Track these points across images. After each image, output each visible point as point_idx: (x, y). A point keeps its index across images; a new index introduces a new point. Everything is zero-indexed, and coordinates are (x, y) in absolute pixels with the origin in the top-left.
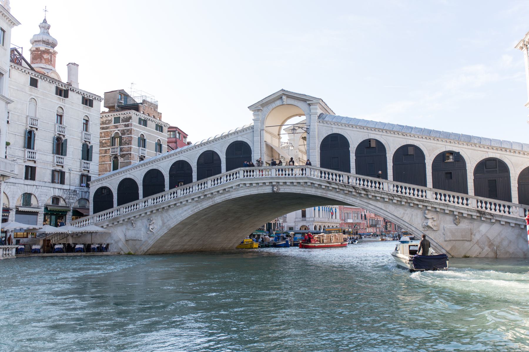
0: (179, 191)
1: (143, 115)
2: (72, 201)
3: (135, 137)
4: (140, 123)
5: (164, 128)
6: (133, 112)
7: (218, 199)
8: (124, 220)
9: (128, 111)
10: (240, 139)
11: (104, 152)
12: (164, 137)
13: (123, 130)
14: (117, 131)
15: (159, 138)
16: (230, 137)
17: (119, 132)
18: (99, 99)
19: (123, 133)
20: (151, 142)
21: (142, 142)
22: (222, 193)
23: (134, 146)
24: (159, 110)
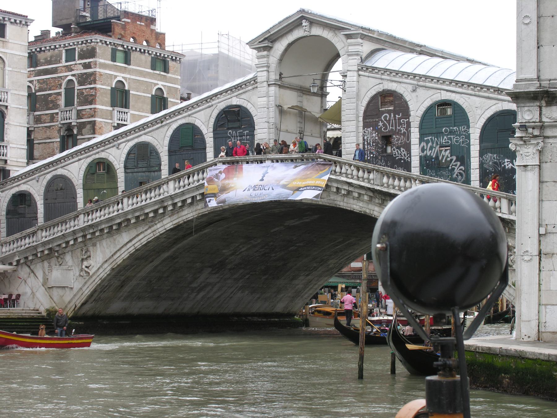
0: (125, 200)
1: (120, 42)
3: (103, 87)
4: (114, 59)
5: (171, 64)
6: (98, 37)
7: (188, 214)
8: (43, 251)
9: (88, 37)
10: (235, 101)
11: (48, 118)
13: (82, 74)
14: (70, 78)
15: (160, 84)
16: (222, 98)
17: (74, 78)
18: (23, 21)
19: (84, 79)
20: (140, 95)
21: (120, 97)
22: (191, 204)
24: (159, 27)
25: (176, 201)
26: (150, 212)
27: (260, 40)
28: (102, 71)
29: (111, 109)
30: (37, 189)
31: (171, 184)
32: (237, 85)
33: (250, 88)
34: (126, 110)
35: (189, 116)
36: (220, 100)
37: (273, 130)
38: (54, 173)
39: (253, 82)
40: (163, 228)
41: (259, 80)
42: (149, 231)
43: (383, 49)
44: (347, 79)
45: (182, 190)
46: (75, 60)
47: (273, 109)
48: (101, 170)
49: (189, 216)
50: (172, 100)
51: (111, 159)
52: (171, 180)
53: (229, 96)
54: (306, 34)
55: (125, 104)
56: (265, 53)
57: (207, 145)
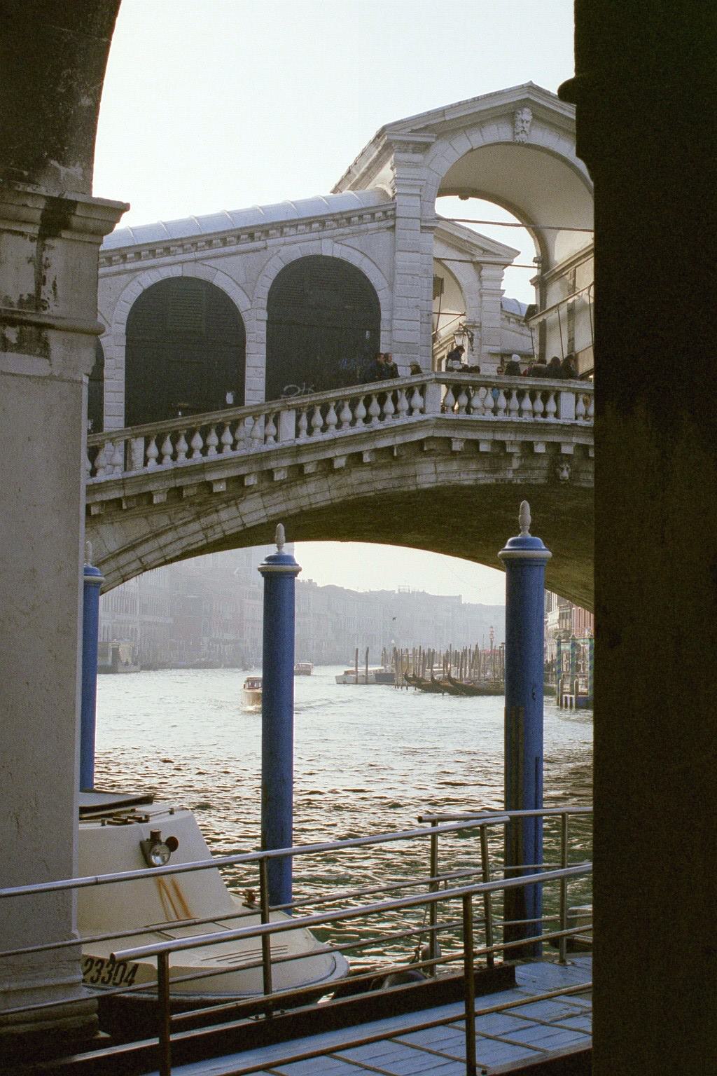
25: (303, 460)
26: (219, 481)
27: (415, 128)
32: (341, 213)
33: (375, 225)
35: (196, 261)
36: (288, 239)
39: (380, 214)
40: (239, 521)
42: (195, 526)
49: (319, 497)
52: (289, 408)
53: (315, 235)
54: (521, 137)
56: (418, 157)
57: (249, 337)
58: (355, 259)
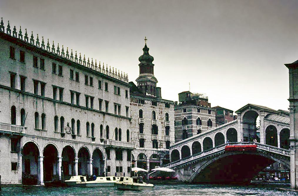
2: (162, 156)
10: (232, 127)
12: (213, 117)
14: (185, 117)
17: (186, 117)
21: (199, 122)
23: (194, 125)
24: (209, 102)
28: (194, 115)
29: (196, 125)
30: (179, 149)
31: (216, 149)
34: (200, 125)
37: (242, 135)
38: (184, 145)
41: (238, 122)
43: (270, 114)
44: (261, 122)
45: (219, 150)
46: (186, 112)
47: (242, 129)
48: (196, 145)
50: (213, 122)
51: (199, 141)
55: (201, 124)
56: (240, 115)
58: (235, 128)
